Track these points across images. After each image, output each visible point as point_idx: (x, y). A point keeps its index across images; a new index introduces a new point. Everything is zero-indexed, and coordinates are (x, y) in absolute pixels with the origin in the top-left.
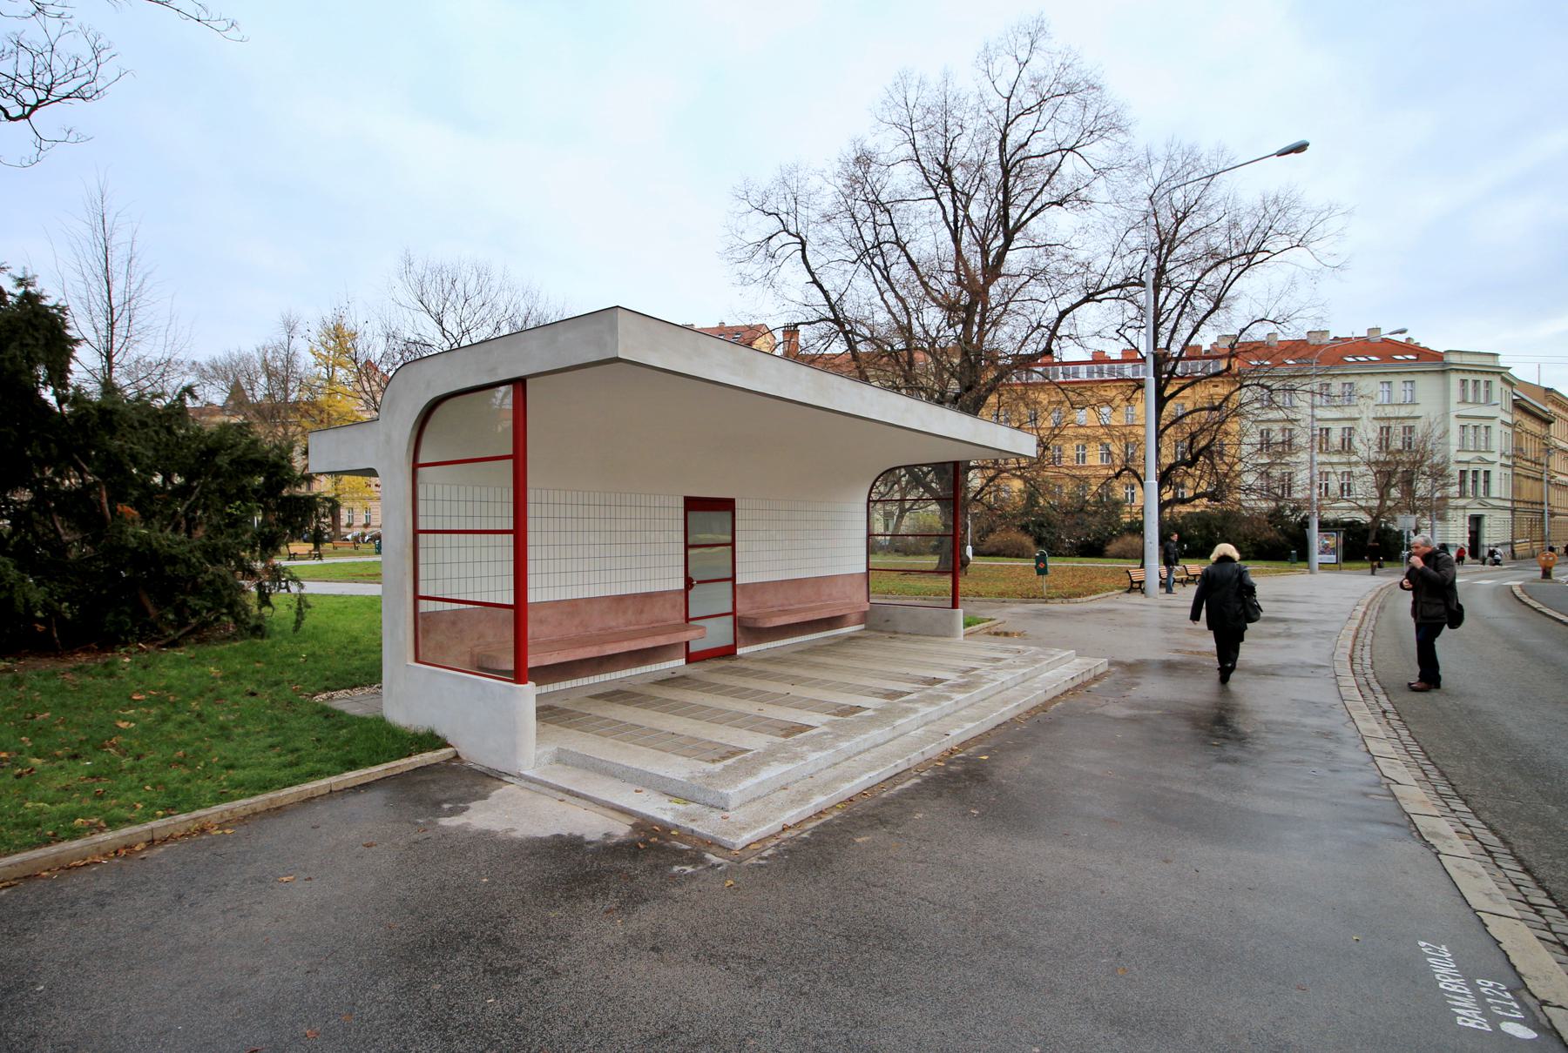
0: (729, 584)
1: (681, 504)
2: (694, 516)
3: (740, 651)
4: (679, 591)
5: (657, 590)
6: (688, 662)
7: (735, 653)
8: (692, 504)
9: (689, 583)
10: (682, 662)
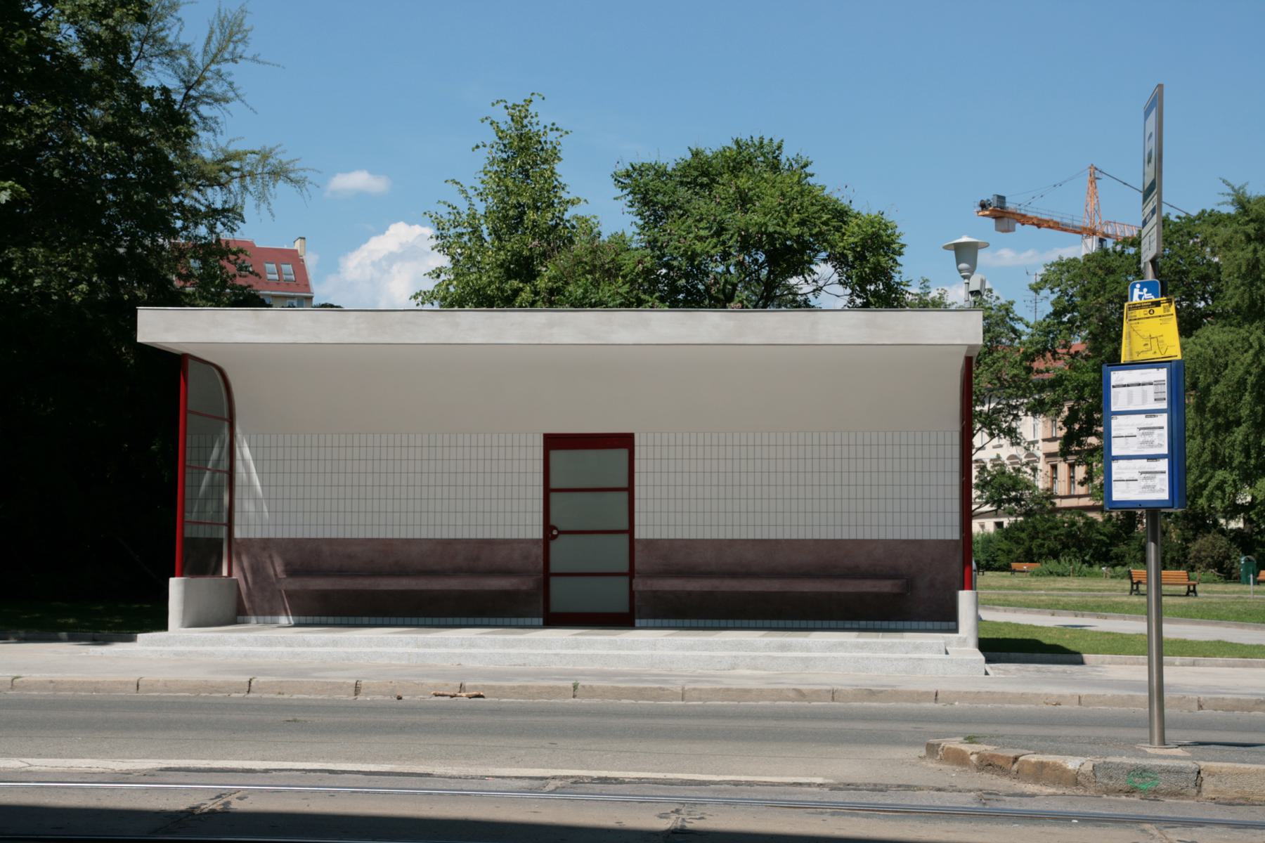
0: (625, 537)
1: (540, 442)
2: (557, 456)
3: (637, 622)
5: (501, 536)
8: (553, 442)
10: (541, 621)
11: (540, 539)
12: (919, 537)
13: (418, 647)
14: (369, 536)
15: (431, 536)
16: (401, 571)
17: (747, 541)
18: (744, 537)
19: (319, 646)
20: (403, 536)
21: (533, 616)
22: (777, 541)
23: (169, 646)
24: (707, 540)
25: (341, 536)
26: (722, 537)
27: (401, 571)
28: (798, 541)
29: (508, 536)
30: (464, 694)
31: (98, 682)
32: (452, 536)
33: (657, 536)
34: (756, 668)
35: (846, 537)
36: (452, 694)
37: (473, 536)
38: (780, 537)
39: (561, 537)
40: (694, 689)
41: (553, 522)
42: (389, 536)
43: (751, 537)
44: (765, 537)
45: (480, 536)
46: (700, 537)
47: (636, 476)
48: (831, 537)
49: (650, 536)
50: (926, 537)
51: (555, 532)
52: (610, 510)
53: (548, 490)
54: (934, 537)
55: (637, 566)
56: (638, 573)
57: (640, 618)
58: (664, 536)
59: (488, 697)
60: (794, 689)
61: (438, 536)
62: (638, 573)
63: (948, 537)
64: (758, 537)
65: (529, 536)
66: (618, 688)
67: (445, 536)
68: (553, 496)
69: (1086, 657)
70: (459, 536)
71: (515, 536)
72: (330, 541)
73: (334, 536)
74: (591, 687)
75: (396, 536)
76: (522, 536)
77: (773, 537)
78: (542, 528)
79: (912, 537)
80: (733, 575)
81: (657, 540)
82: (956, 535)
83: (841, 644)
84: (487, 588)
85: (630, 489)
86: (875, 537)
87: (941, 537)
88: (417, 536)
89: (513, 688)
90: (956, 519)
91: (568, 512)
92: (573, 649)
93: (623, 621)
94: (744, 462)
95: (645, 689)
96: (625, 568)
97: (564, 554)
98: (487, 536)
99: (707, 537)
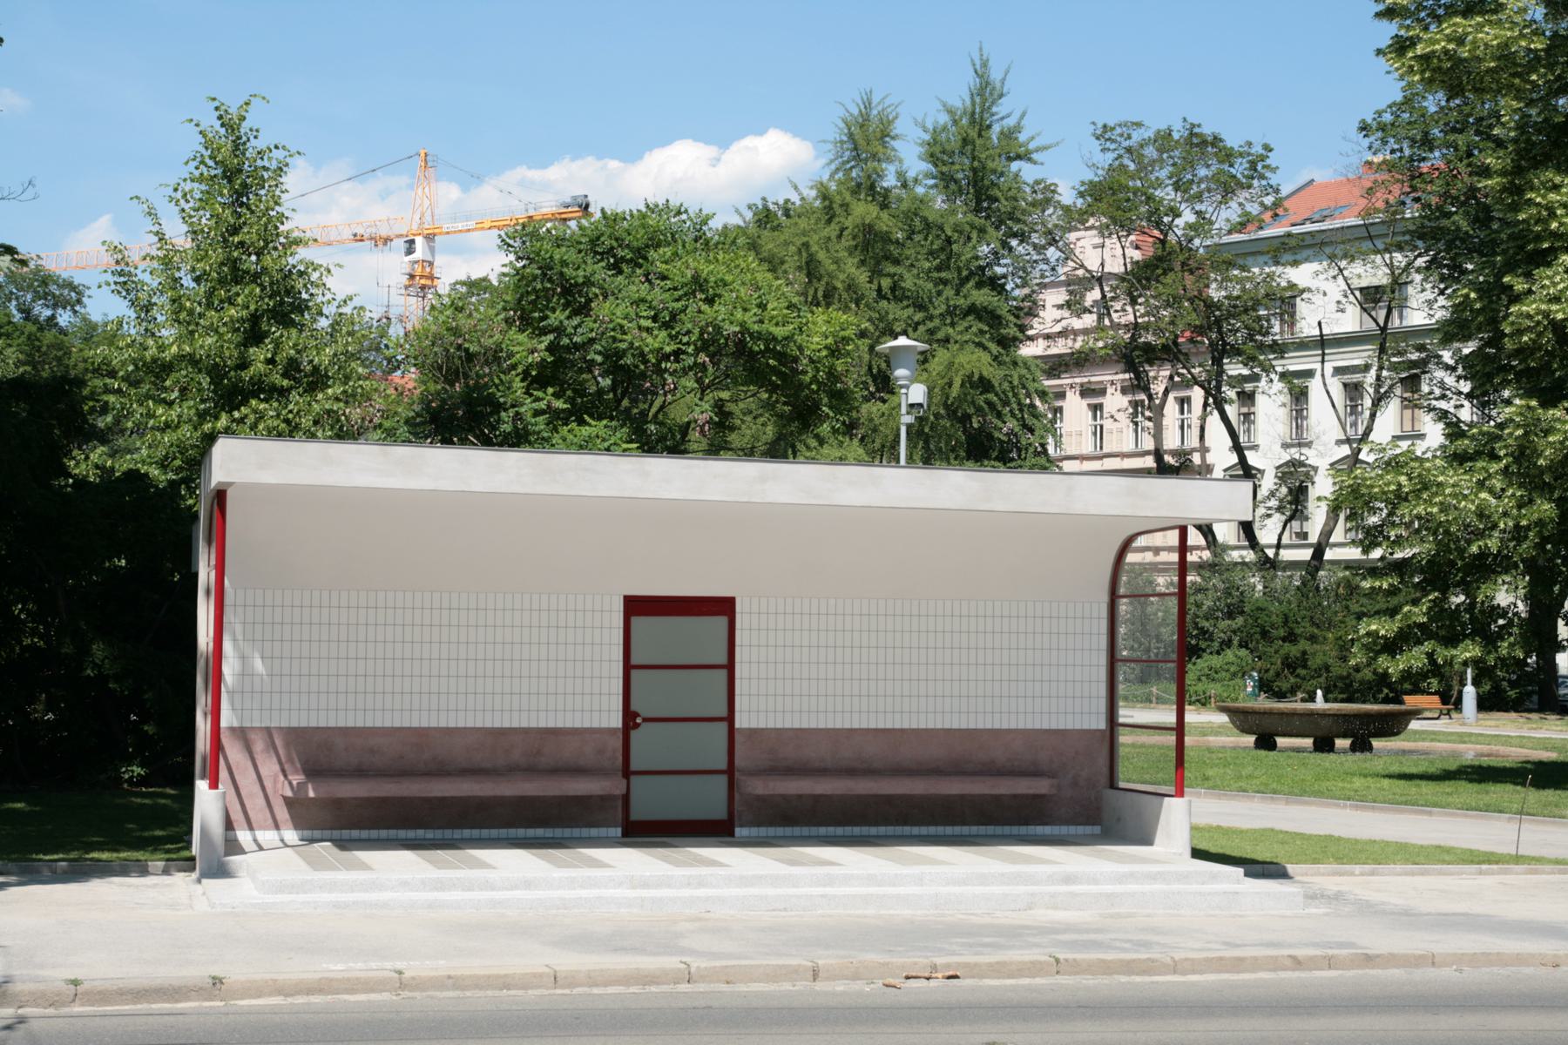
0: (723, 726)
1: (619, 606)
3: (740, 832)
4: (611, 731)
5: (569, 725)
6: (625, 834)
7: (732, 834)
8: (636, 606)
9: (629, 716)
10: (619, 831)
11: (617, 729)
12: (1062, 727)
13: (634, 888)
14: (397, 724)
15: (480, 725)
16: (440, 770)
17: (868, 730)
18: (864, 726)
19: (507, 889)
20: (443, 724)
21: (608, 826)
22: (902, 731)
23: (306, 893)
25: (360, 724)
26: (839, 726)
27: (440, 770)
28: (926, 730)
29: (578, 725)
30: (940, 975)
31: (506, 976)
32: (506, 725)
33: (762, 725)
34: (1055, 908)
35: (980, 726)
36: (927, 975)
37: (533, 725)
38: (906, 726)
39: (645, 725)
40: (1186, 959)
41: (634, 707)
42: (425, 724)
43: (873, 726)
44: (889, 726)
45: (542, 725)
46: (813, 726)
47: (738, 650)
48: (964, 726)
49: (754, 725)
50: (1070, 727)
51: (639, 720)
52: (704, 693)
53: (628, 667)
54: (1078, 727)
55: (738, 762)
57: (741, 826)
58: (771, 725)
59: (965, 978)
60: (1290, 956)
61: (488, 725)
63: (1094, 727)
64: (881, 726)
65: (605, 725)
66: (1103, 961)
67: (497, 725)
68: (634, 674)
69: (1290, 868)
70: (515, 725)
71: (587, 725)
72: (345, 732)
73: (351, 724)
74: (1075, 960)
75: (434, 724)
76: (596, 725)
77: (897, 726)
78: (621, 714)
79: (1054, 726)
80: (851, 772)
82: (1102, 724)
83: (1132, 875)
84: (571, 793)
85: (730, 667)
86: (1013, 726)
87: (1086, 727)
88: (461, 724)
89: (990, 965)
90: (1102, 705)
91: (653, 695)
92: (825, 886)
93: (717, 830)
94: (931, 652)
95: (1134, 961)
96: (723, 765)
97: (648, 746)
98: (551, 725)
99: (822, 726)
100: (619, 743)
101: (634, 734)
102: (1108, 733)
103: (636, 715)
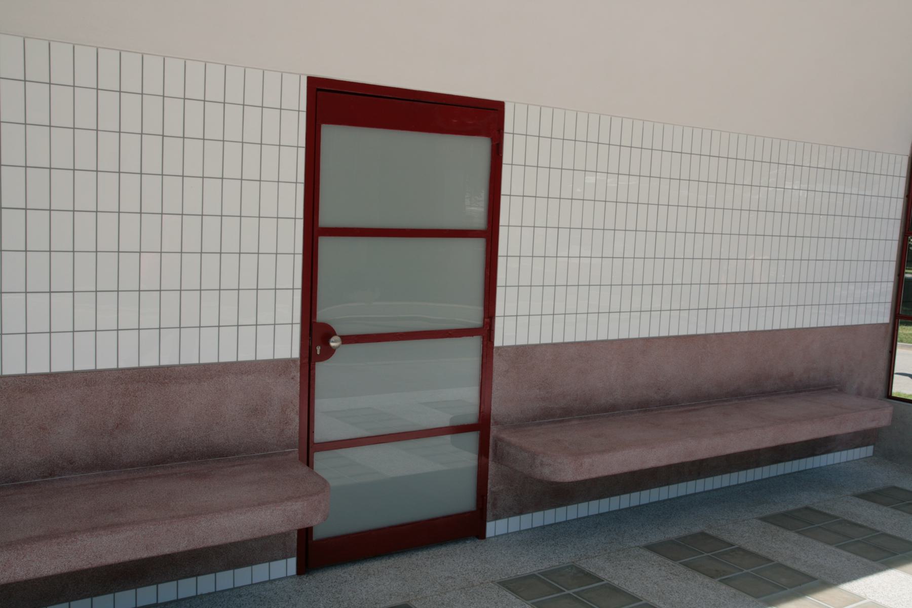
0: (474, 344)
3: (493, 528)
4: (278, 366)
6: (303, 569)
7: (480, 534)
11: (293, 361)
17: (668, 338)
22: (706, 337)
24: (612, 342)
29: (209, 357)
37: (107, 362)
41: (323, 315)
45: (128, 361)
51: (334, 343)
55: (497, 408)
56: (496, 423)
57: (497, 517)
62: (496, 423)
65: (265, 354)
68: (325, 244)
71: (228, 357)
78: (297, 329)
81: (536, 346)
100: (291, 389)
101: (321, 368)
102: (890, 328)
103: (328, 332)
